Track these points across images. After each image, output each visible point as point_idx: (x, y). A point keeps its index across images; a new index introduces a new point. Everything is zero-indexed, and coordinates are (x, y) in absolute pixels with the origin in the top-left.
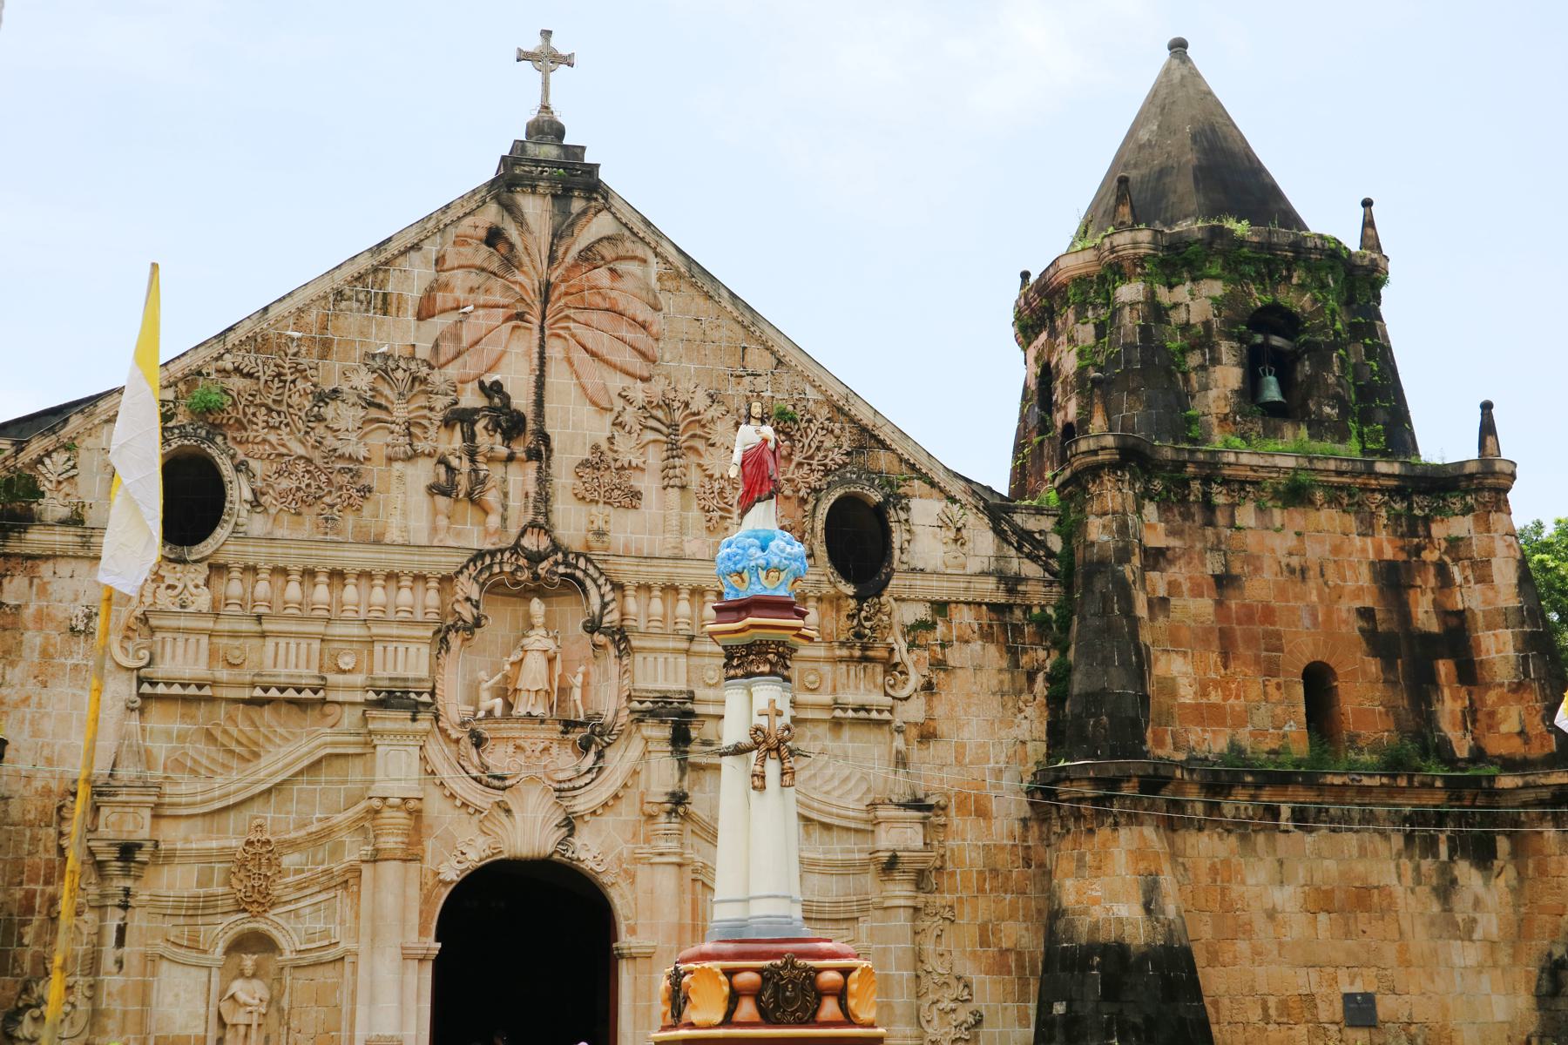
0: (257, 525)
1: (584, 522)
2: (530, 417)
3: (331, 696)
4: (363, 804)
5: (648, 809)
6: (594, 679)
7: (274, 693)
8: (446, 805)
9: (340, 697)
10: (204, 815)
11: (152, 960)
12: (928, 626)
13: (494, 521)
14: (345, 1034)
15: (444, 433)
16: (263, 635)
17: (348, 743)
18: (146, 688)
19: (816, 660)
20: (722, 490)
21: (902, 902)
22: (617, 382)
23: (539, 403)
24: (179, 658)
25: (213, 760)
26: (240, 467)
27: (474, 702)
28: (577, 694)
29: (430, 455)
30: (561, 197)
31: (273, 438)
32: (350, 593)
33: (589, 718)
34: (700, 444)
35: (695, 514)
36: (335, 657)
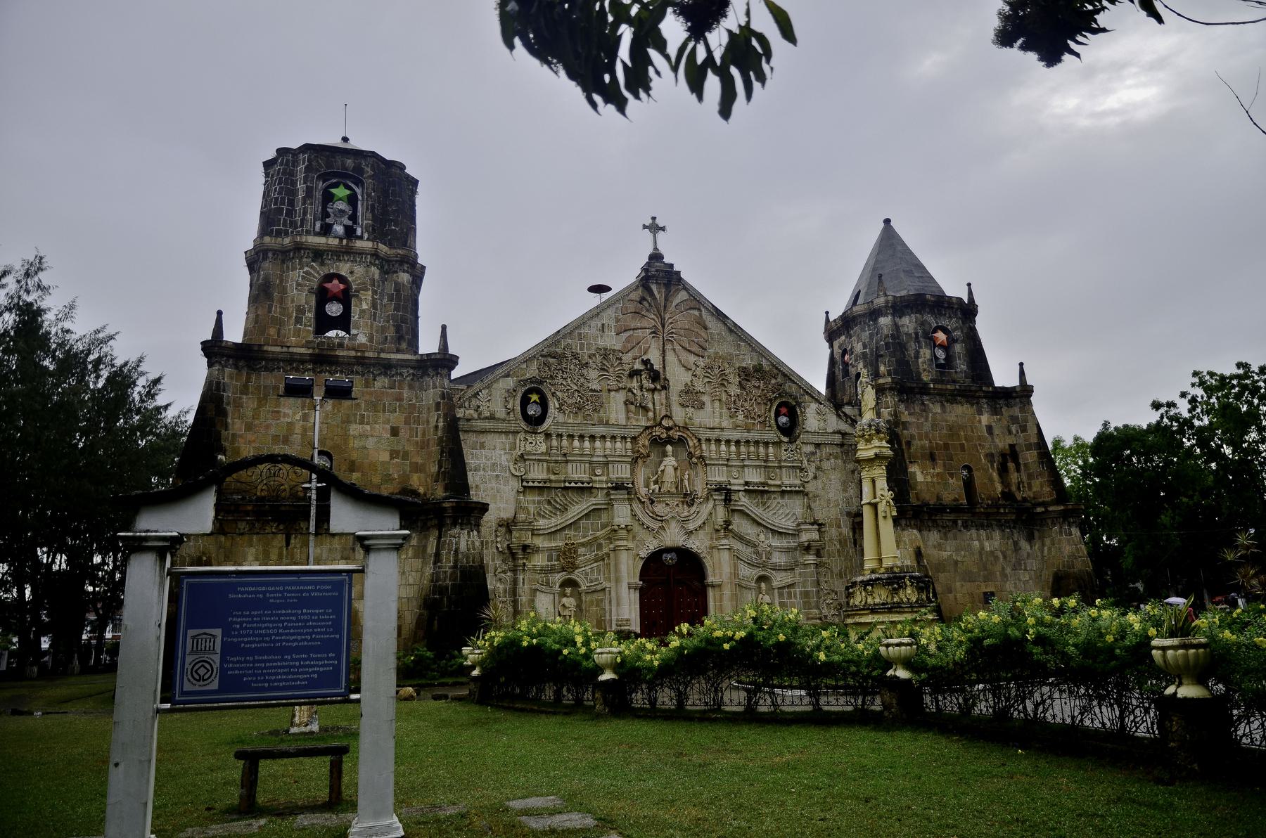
0: (561, 418)
1: (683, 415)
2: (662, 373)
3: (595, 485)
4: (609, 528)
5: (716, 527)
6: (692, 477)
7: (573, 485)
8: (640, 528)
9: (598, 486)
10: (548, 534)
12: (813, 454)
13: (651, 414)
14: (608, 618)
15: (629, 381)
16: (567, 462)
17: (602, 504)
18: (525, 484)
19: (774, 467)
20: (735, 401)
21: (812, 562)
22: (692, 358)
23: (664, 367)
24: (536, 472)
25: (551, 512)
26: (554, 394)
27: (647, 486)
28: (686, 483)
29: (625, 389)
30: (668, 285)
31: (564, 383)
32: (598, 444)
33: (691, 494)
34: (725, 383)
35: (725, 410)
36: (593, 470)
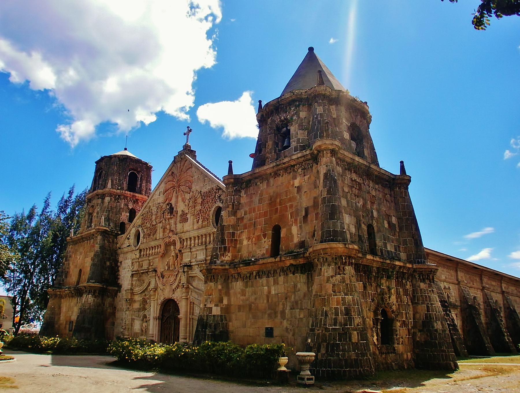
11: (133, 320)
